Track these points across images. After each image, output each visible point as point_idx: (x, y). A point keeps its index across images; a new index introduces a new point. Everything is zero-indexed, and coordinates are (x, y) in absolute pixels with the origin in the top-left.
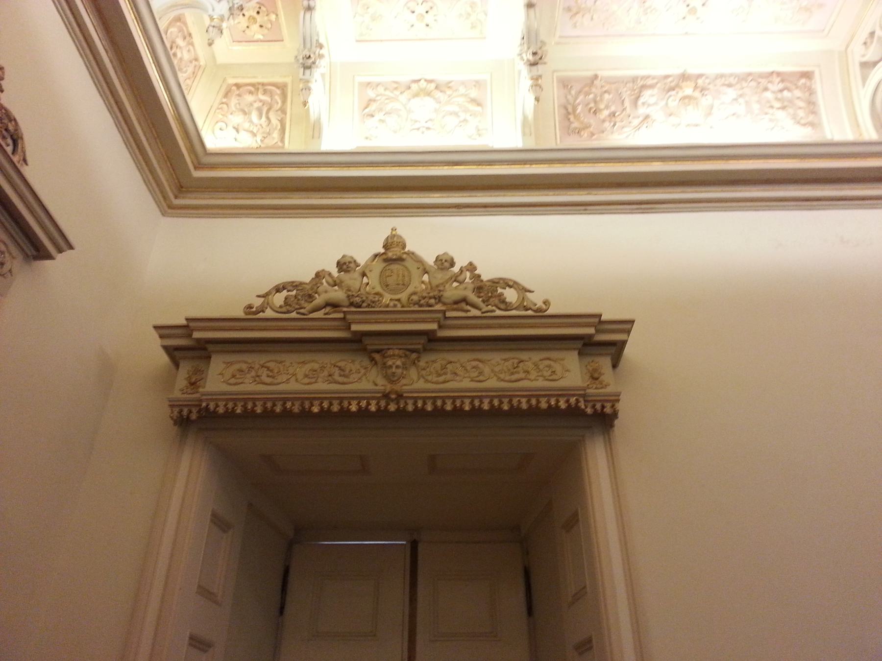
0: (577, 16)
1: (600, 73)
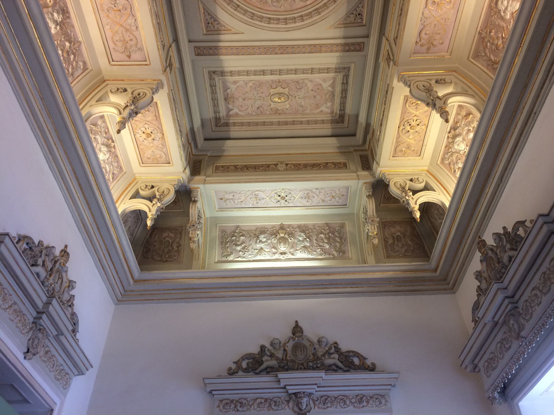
0: (434, 43)
1: (478, 30)
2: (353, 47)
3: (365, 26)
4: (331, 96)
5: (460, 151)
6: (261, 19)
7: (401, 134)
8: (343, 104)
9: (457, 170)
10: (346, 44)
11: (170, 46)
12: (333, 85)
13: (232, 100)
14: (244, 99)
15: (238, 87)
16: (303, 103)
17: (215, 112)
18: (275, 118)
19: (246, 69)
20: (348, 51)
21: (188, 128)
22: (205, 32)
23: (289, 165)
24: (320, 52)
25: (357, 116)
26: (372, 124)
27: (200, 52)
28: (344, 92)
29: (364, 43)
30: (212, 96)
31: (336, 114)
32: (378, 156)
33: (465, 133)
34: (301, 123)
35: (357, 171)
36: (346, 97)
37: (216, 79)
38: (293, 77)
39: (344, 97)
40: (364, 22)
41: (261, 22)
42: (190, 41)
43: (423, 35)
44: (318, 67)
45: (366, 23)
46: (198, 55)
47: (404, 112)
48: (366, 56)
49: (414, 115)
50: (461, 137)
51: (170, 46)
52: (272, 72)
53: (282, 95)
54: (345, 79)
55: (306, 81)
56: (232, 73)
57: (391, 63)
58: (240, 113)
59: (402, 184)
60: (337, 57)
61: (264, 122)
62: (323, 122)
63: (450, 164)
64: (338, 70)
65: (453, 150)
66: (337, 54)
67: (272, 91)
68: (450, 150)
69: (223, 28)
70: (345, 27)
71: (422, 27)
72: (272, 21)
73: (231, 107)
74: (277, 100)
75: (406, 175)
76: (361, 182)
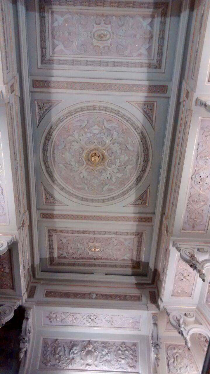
2: (42, 84)
4: (55, 34)
6: (112, 111)
10: (49, 87)
12: (54, 46)
13: (146, 36)
14: (135, 36)
15: (138, 50)
16: (80, 28)
19: (129, 68)
20: (46, 81)
21: (195, 11)
22: (155, 103)
24: (67, 83)
25: (27, 9)
26: (11, 5)
28: (43, 40)
29: (33, 87)
31: (48, 11)
37: (156, 61)
39: (43, 32)
40: (36, 102)
41: (112, 109)
42: (169, 98)
45: (35, 102)
46: (164, 86)
48: (31, 75)
52: (107, 64)
53: (100, 39)
54: (44, 51)
56: (141, 65)
58: (140, 19)
60: (52, 76)
61: (118, 7)
64: (51, 62)
66: (53, 79)
69: (141, 106)
70: (50, 100)
72: (104, 109)
73: (149, 28)
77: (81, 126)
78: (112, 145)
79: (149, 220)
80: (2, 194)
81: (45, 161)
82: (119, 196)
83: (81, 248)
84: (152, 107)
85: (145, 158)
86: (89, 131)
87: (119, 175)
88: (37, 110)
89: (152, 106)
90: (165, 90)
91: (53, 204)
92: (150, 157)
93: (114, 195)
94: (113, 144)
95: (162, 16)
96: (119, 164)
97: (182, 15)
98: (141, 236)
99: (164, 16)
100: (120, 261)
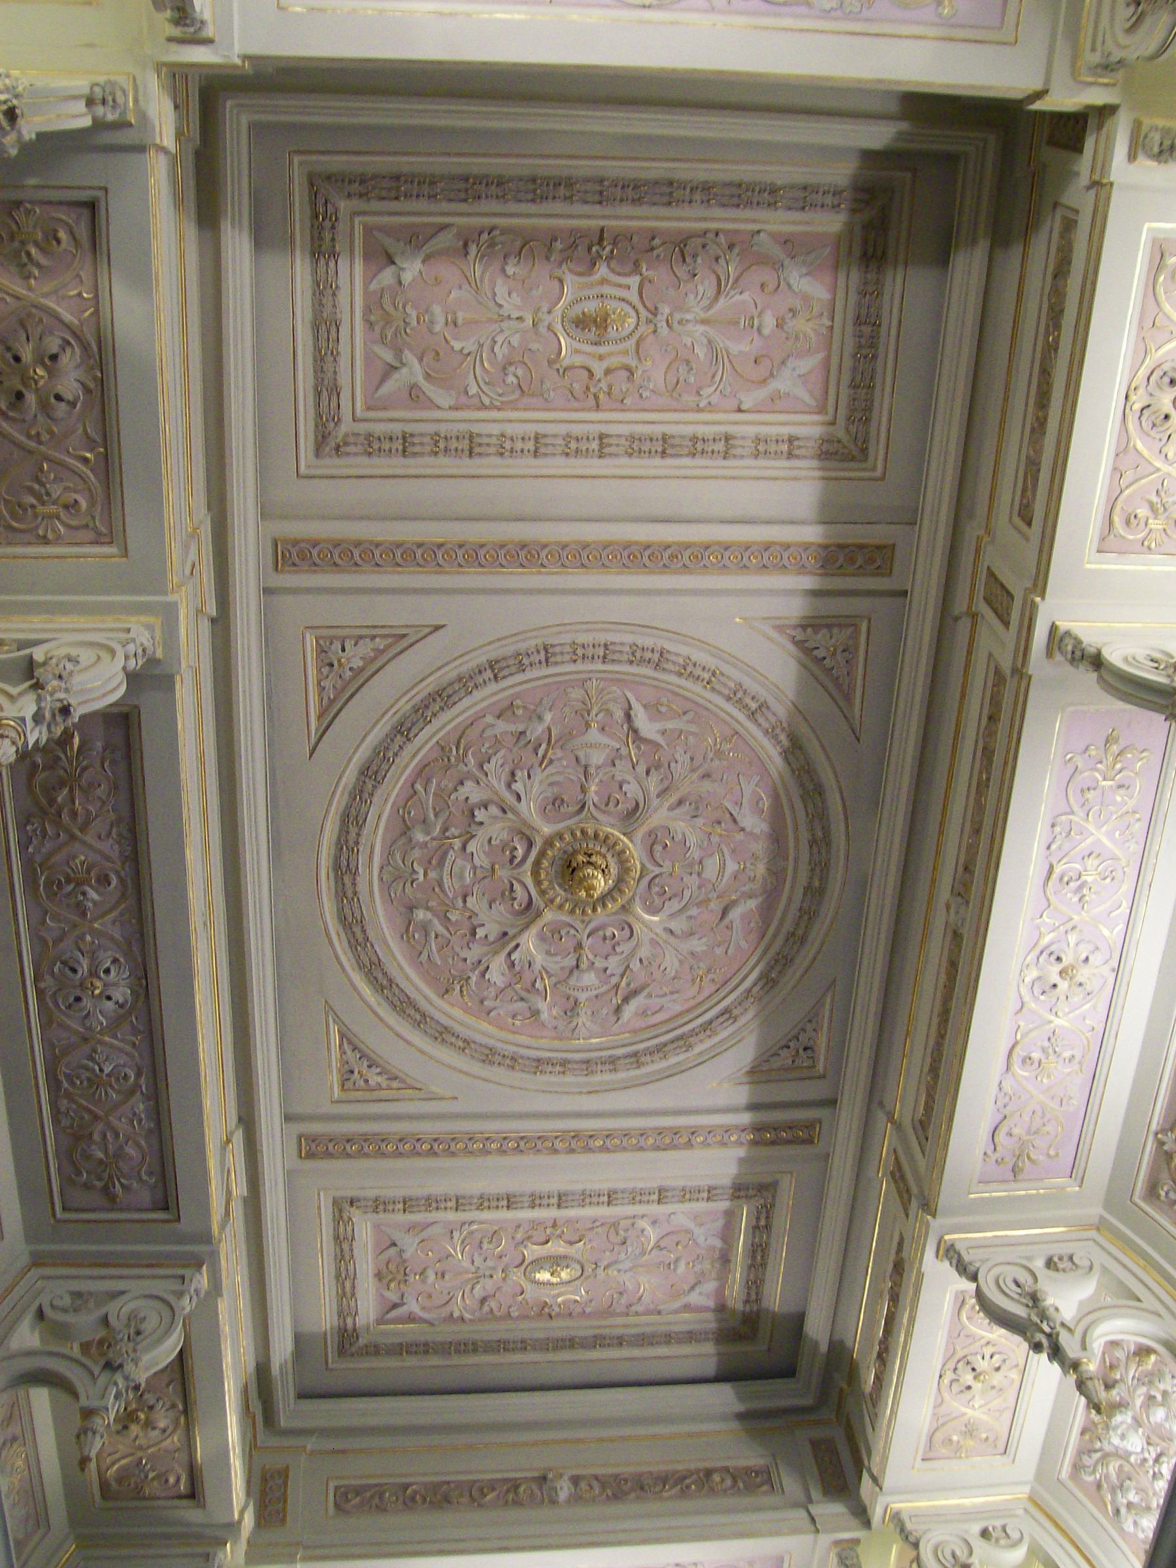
1: (1154, 1127)
3: (824, 1077)
5: (1130, 1454)
7: (946, 1395)
8: (755, 1286)
9: (1123, 1511)
11: (229, 1141)
17: (340, 1314)
18: (538, 1330)
20: (773, 1143)
23: (583, 1485)
24: (689, 1145)
27: (314, 1148)
30: (338, 1269)
32: (876, 1458)
33: (1139, 1402)
34: (620, 1342)
35: (810, 1501)
36: (764, 1265)
38: (603, 1211)
40: (820, 1067)
42: (288, 1118)
43: (1001, 1137)
44: (681, 1183)
45: (825, 1068)
46: (311, 1155)
47: (957, 1332)
49: (983, 1341)
50: (1130, 1414)
51: (229, 1141)
55: (642, 1224)
57: (914, 1204)
59: (958, 1553)
62: (691, 1337)
63: (1099, 1486)
64: (740, 1190)
65: (1107, 1448)
67: (532, 1251)
68: (1098, 1445)
71: (1001, 1117)
74: (544, 1276)
75: (968, 1515)
76: (825, 1539)
77: (650, 996)
78: (511, 932)
79: (290, 555)
80: (1051, 868)
81: (821, 842)
82: (467, 683)
83: (690, 327)
84: (348, 1079)
85: (354, 884)
86: (614, 980)
87: (471, 792)
88: (822, 1042)
89: (349, 1085)
90: (307, 1144)
91: (818, 621)
92: (326, 885)
93: (493, 687)
94: (505, 934)
95: (355, 1330)
96: (472, 847)
97: (289, 1346)
98: (322, 440)
99: (346, 1330)
100: (443, 227)
